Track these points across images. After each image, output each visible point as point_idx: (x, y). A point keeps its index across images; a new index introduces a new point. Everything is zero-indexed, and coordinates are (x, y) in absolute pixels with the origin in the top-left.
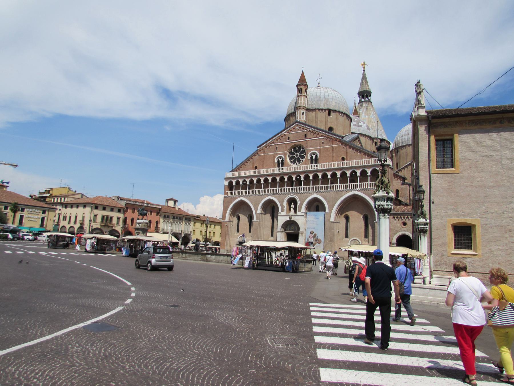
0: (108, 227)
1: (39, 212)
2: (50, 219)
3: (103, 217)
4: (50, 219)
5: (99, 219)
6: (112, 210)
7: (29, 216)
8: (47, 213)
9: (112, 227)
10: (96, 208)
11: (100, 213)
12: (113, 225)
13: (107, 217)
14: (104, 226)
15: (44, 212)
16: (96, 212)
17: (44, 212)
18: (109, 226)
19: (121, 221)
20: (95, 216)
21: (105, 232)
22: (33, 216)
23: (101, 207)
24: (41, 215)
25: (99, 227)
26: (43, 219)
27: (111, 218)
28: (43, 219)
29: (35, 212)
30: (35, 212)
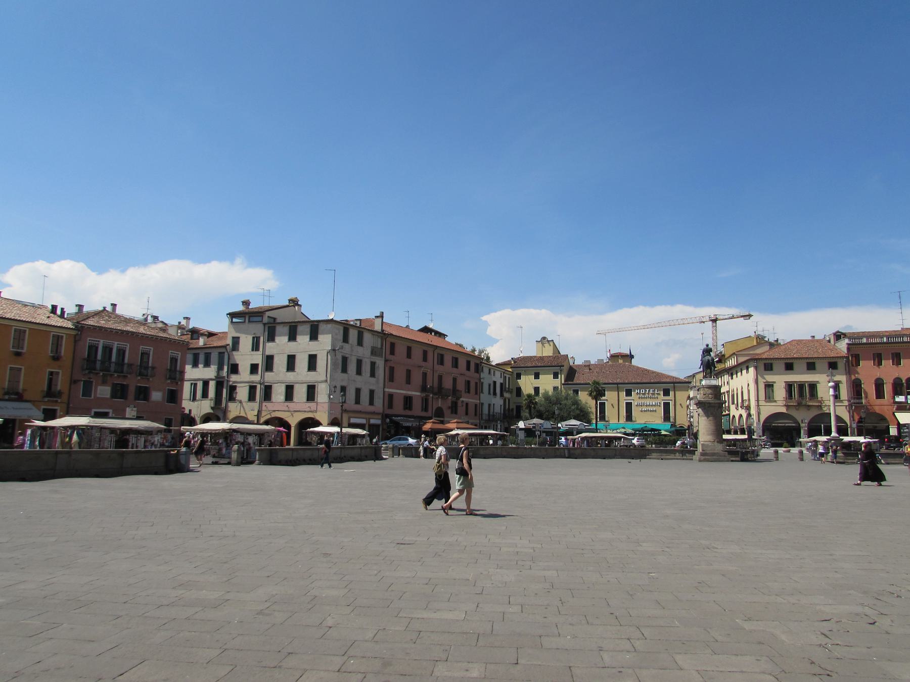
0: (809, 410)
1: (658, 394)
2: (681, 405)
3: (789, 386)
4: (681, 405)
5: (780, 393)
6: (811, 367)
7: (641, 401)
8: (672, 393)
9: (820, 407)
10: (768, 367)
11: (780, 380)
12: (820, 402)
13: (801, 386)
14: (799, 405)
15: (666, 393)
16: (770, 378)
17: (666, 393)
18: (809, 406)
19: (844, 393)
20: (769, 386)
21: (800, 423)
22: (648, 402)
23: (779, 366)
24: (662, 399)
25: (784, 410)
26: (667, 406)
27: (813, 386)
28: (667, 406)
29: (650, 395)
30: (650, 395)
